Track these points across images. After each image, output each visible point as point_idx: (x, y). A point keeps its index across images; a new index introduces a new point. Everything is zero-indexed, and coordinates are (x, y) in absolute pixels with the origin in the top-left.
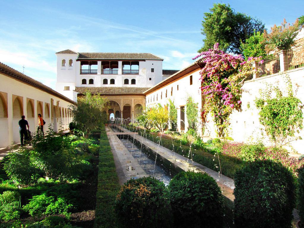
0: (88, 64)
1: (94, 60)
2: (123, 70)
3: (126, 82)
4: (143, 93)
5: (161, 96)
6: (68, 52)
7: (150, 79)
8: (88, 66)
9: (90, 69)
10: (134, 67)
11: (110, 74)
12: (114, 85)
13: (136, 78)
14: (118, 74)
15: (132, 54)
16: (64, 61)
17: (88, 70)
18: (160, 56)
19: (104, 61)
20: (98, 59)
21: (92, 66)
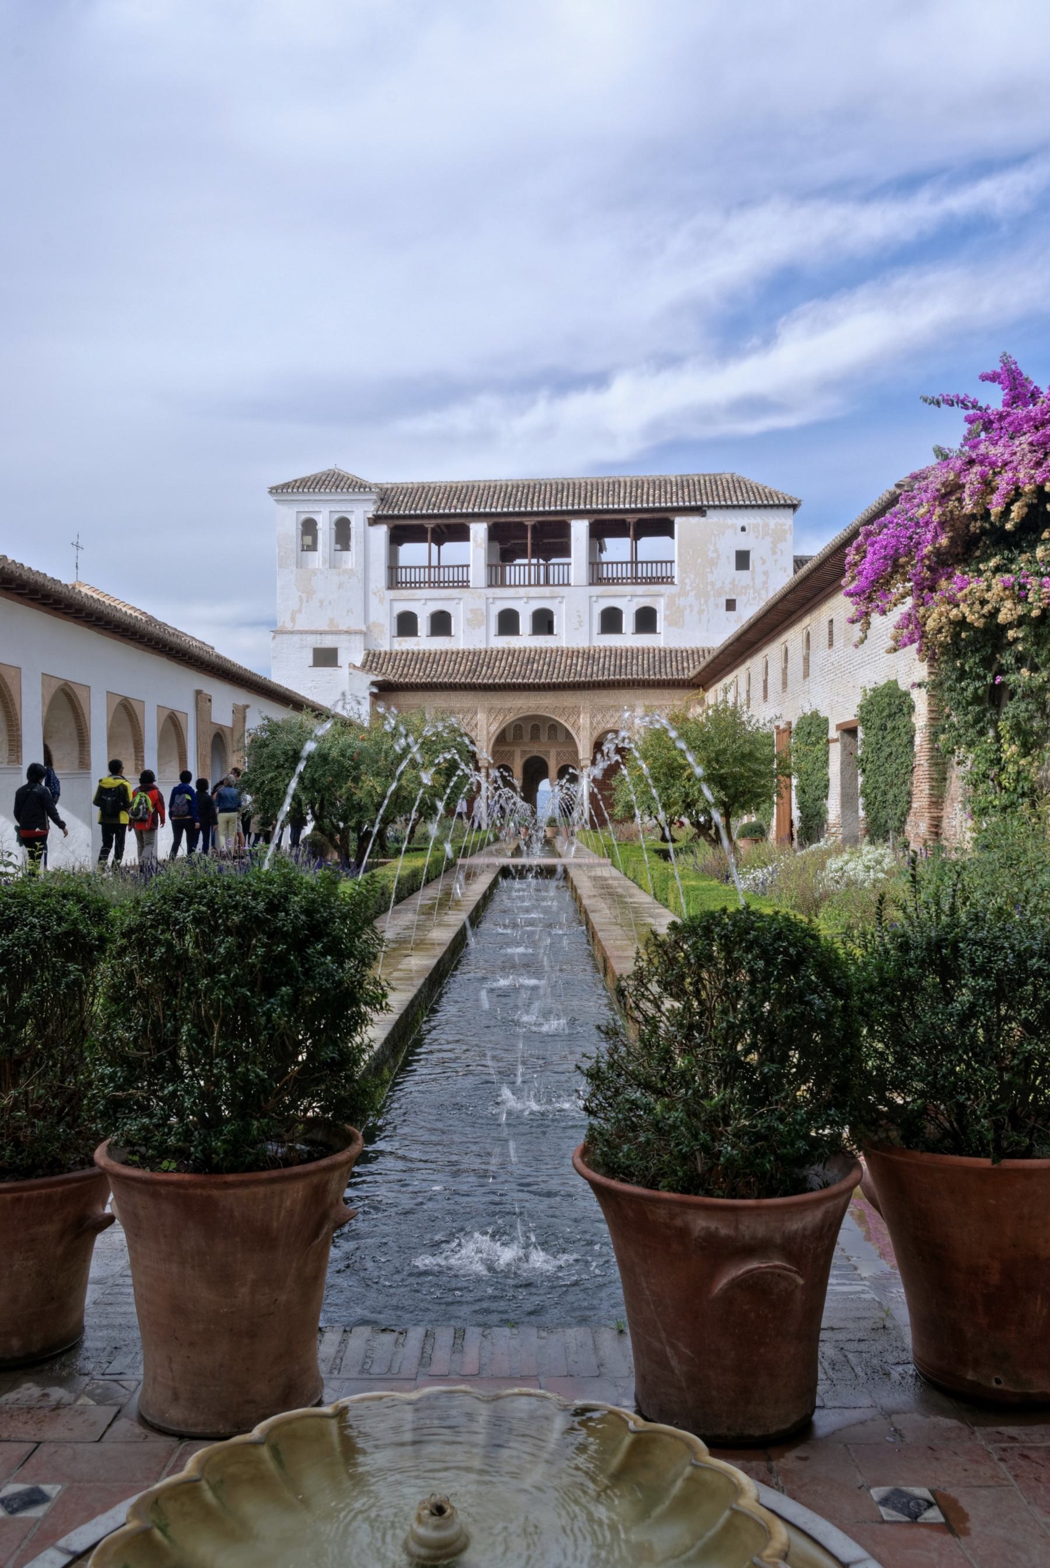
0: (423, 540)
1: (455, 515)
2: (594, 563)
3: (611, 620)
4: (692, 673)
5: (765, 681)
6: (332, 482)
7: (731, 605)
8: (424, 546)
9: (434, 563)
10: (651, 546)
11: (530, 585)
12: (548, 637)
13: (660, 600)
14: (569, 585)
15: (638, 485)
16: (309, 527)
17: (424, 567)
18: (788, 490)
19: (503, 520)
20: (470, 510)
21: (448, 547)
